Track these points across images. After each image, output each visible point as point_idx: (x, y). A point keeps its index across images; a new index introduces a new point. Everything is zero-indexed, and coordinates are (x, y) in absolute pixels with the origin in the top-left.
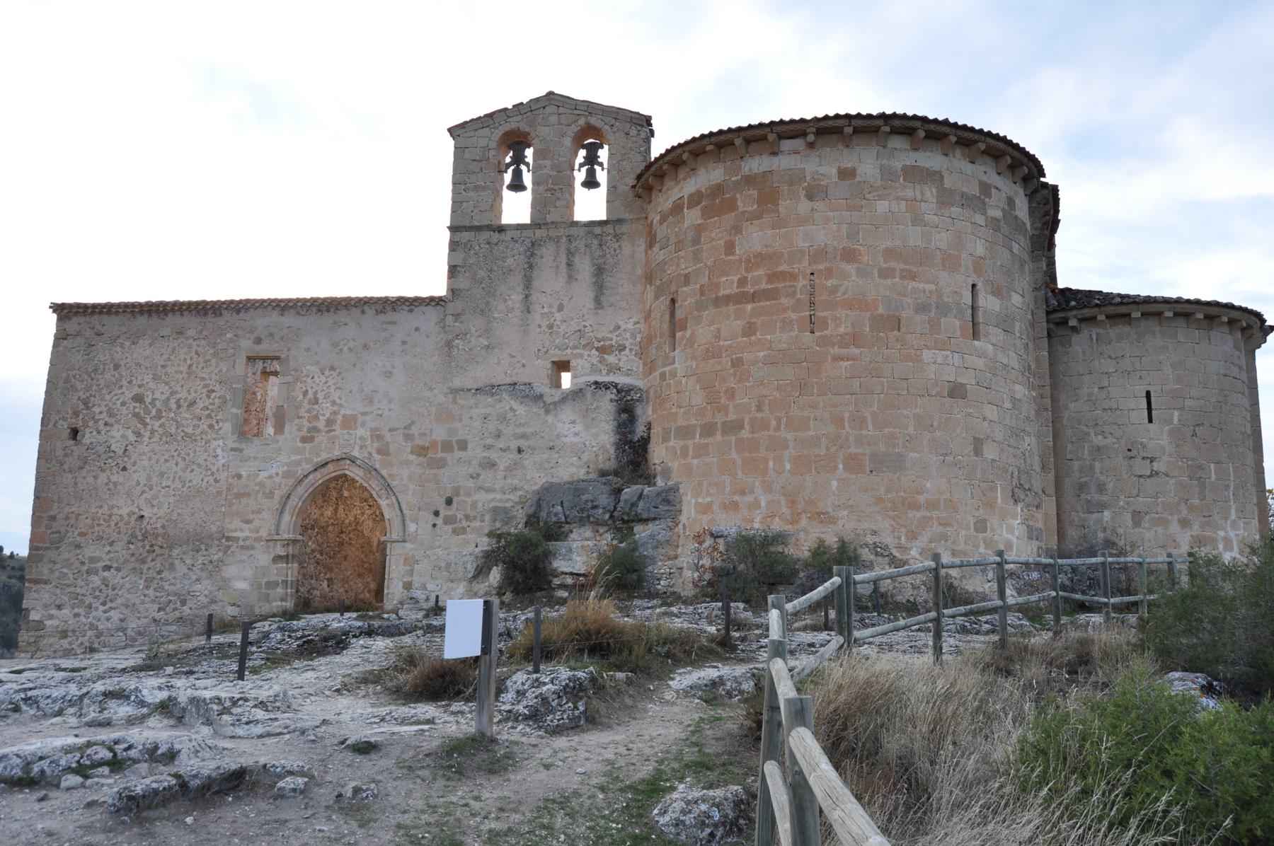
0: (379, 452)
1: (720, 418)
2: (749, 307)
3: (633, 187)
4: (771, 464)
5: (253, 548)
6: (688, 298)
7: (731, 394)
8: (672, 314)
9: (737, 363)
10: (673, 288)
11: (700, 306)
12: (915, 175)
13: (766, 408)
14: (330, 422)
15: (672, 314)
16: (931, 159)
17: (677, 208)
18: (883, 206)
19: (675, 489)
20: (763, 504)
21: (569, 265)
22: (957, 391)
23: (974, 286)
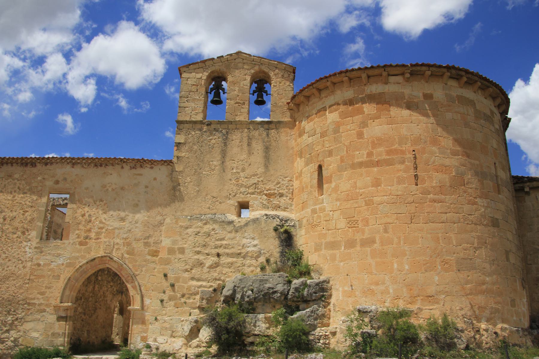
1: (358, 237)
2: (375, 169)
3: (288, 103)
4: (395, 266)
5: (44, 311)
6: (331, 166)
7: (366, 222)
9: (369, 203)
10: (320, 158)
11: (341, 169)
12: (462, 100)
13: (390, 230)
14: (98, 234)
16: (469, 93)
20: (391, 291)
21: (249, 145)
23: (495, 163)
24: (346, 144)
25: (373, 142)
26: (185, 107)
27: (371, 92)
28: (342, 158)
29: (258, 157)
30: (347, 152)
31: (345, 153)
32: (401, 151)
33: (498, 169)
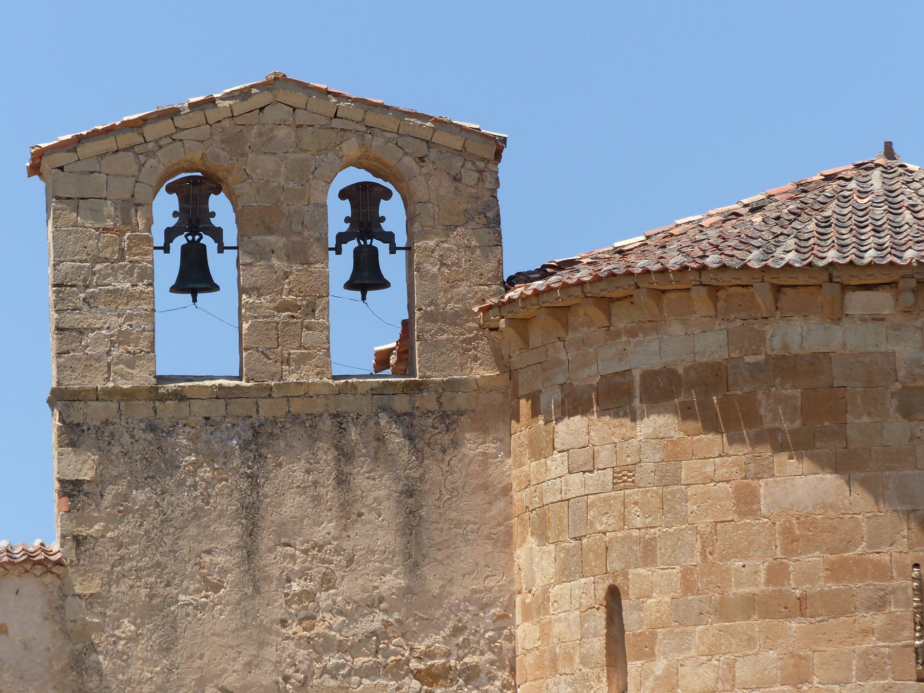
6: (652, 597)
10: (616, 565)
21: (342, 481)
24: (701, 527)
25: (787, 531)
26: (81, 332)
27: (785, 346)
28: (687, 573)
29: (379, 531)
30: (705, 558)
31: (698, 559)
32: (877, 565)
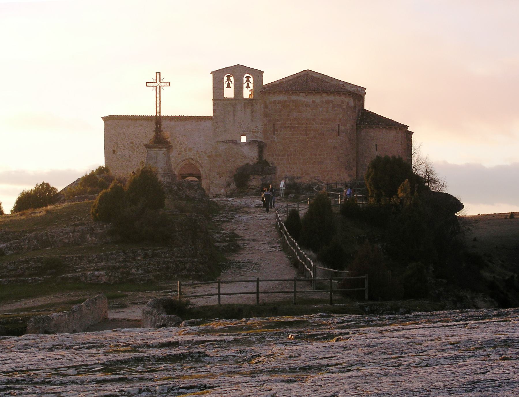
0: (199, 157)
8: (274, 127)
14: (185, 149)
15: (274, 127)
17: (274, 102)
18: (321, 109)
19: (275, 167)
22: (335, 148)
33: (340, 126)
